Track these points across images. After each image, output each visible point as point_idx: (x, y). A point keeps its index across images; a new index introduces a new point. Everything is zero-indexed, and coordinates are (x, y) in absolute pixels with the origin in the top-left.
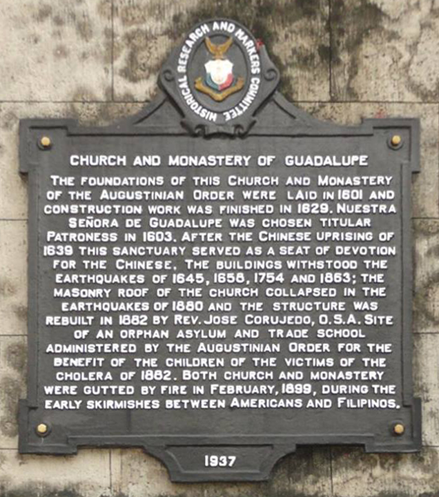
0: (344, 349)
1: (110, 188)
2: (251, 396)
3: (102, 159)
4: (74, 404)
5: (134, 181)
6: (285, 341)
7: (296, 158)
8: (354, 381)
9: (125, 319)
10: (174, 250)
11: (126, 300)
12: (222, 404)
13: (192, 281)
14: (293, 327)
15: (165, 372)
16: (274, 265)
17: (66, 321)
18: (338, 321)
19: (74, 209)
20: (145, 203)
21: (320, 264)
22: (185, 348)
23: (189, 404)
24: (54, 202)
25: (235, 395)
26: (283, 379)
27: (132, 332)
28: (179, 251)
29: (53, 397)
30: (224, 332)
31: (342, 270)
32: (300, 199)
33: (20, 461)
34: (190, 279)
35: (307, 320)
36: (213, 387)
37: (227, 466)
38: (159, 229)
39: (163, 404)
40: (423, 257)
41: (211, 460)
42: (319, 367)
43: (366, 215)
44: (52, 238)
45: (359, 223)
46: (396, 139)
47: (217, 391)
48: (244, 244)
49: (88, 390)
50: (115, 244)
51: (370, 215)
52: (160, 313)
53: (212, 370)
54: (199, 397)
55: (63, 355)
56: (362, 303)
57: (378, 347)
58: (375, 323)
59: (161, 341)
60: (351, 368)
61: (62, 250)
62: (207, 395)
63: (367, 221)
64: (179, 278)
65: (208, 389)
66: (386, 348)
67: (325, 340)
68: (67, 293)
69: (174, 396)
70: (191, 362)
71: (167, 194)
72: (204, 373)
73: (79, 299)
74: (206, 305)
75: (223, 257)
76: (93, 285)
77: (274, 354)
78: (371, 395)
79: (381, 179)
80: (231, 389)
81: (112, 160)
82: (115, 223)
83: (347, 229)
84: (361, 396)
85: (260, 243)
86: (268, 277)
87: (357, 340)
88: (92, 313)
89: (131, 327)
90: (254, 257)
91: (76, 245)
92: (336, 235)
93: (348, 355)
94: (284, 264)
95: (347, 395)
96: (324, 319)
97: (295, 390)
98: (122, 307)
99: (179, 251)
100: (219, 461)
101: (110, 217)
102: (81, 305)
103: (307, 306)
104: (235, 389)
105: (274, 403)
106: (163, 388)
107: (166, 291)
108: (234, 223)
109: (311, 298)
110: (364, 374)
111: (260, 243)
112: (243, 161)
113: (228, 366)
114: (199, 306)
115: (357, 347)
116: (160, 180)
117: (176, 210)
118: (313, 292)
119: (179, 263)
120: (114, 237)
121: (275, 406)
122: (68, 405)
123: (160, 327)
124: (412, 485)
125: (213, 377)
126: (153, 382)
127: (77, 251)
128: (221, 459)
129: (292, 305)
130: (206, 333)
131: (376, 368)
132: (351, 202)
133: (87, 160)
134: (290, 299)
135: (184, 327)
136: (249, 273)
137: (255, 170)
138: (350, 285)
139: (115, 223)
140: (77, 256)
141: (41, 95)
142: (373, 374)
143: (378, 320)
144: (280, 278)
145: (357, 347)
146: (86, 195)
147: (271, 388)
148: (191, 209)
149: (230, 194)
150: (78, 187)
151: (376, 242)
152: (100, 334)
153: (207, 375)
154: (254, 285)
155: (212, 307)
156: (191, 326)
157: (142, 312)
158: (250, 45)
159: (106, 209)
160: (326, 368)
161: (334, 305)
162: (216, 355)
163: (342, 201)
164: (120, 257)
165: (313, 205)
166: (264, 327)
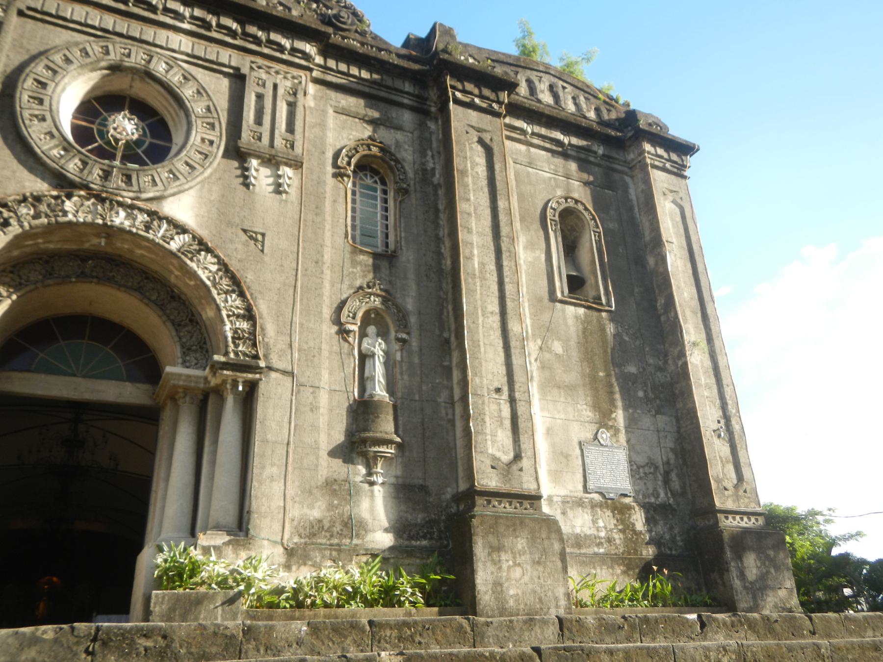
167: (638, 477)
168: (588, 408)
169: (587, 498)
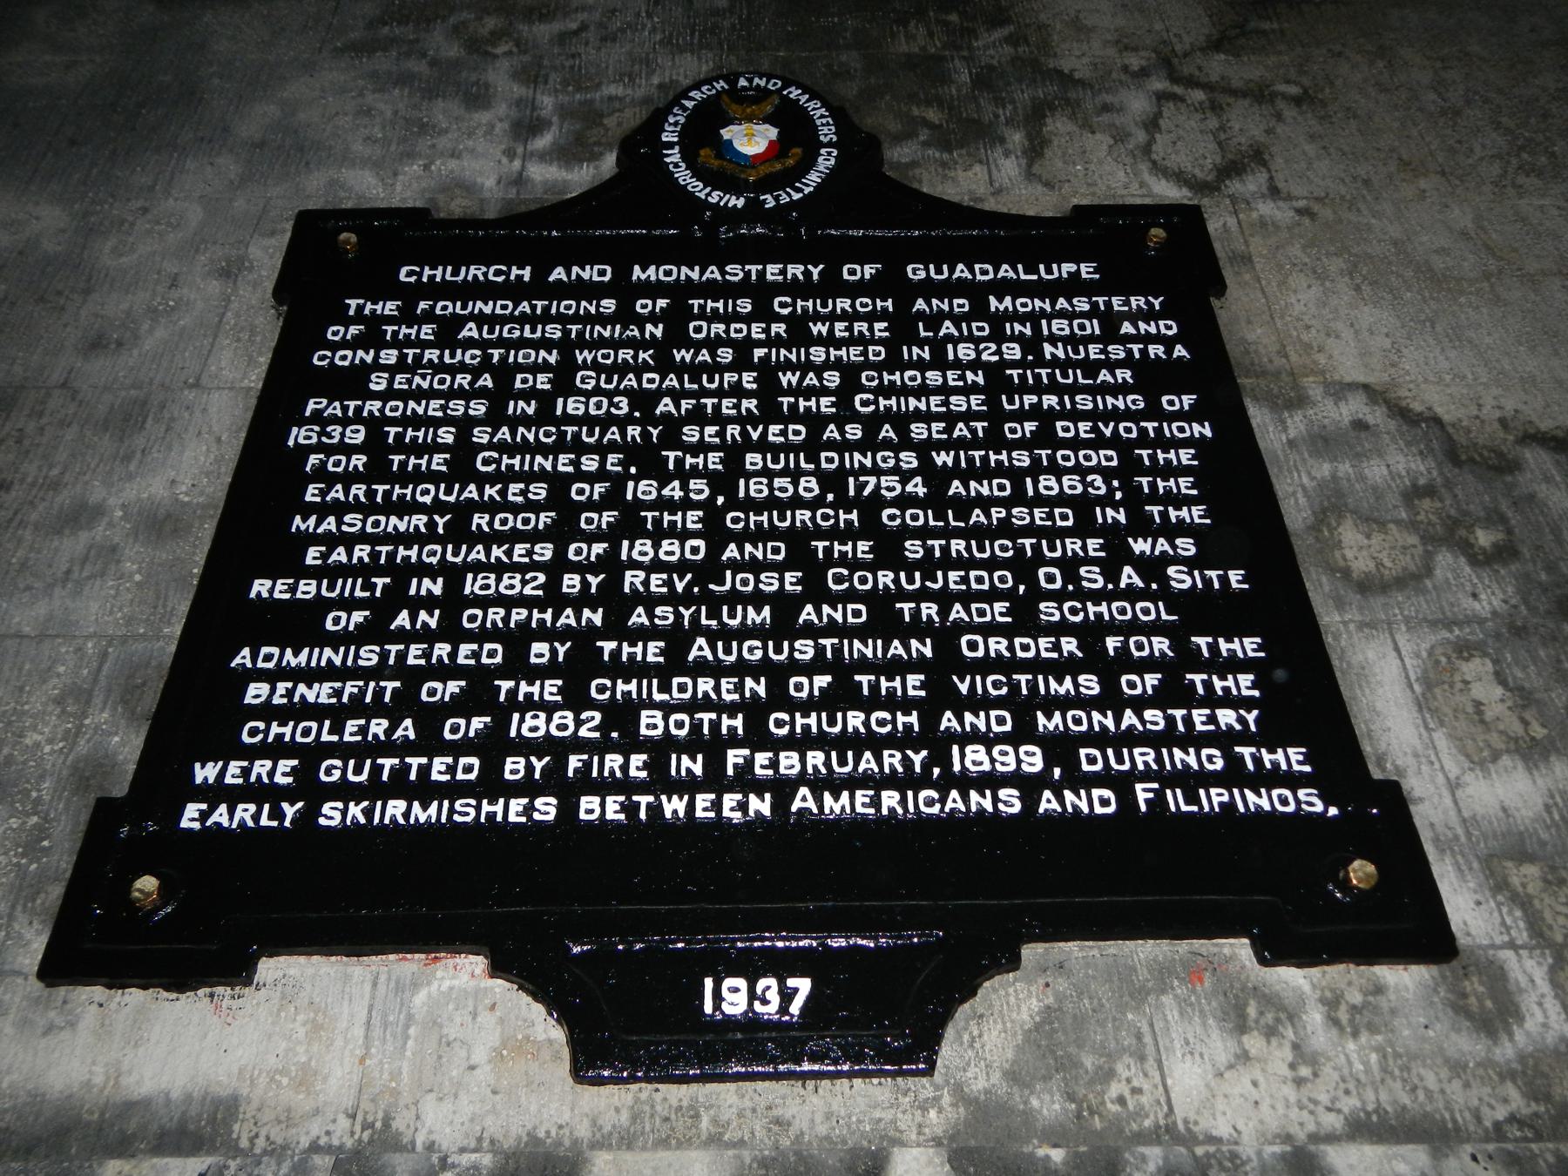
1: (481, 319)
2: (854, 783)
3: (475, 271)
4: (277, 814)
6: (947, 636)
12: (761, 805)
14: (967, 598)
15: (584, 716)
16: (898, 460)
17: (307, 589)
19: (390, 356)
21: (1022, 459)
22: (653, 652)
25: (802, 779)
27: (496, 615)
29: (218, 794)
30: (766, 611)
34: (674, 490)
35: (1004, 579)
36: (734, 757)
38: (597, 391)
39: (568, 809)
41: (725, 993)
42: (1057, 696)
44: (317, 414)
45: (1104, 376)
48: (815, 422)
49: (331, 771)
51: (1127, 362)
52: (581, 569)
53: (732, 710)
54: (689, 786)
55: (281, 673)
57: (1224, 646)
59: (584, 639)
60: (1159, 699)
61: (337, 435)
62: (715, 780)
63: (1124, 375)
65: (715, 763)
66: (1249, 646)
67: (1062, 628)
68: (330, 524)
69: (603, 787)
73: (363, 537)
74: (715, 549)
75: (763, 446)
76: (405, 508)
77: (918, 665)
78: (1234, 776)
80: (789, 762)
82: (487, 381)
84: (1208, 779)
85: (856, 417)
86: (884, 484)
87: (1155, 629)
88: (391, 568)
90: (843, 446)
91: (375, 426)
92: (1050, 400)
96: (1050, 579)
97: (993, 761)
98: (478, 554)
99: (645, 435)
102: (362, 552)
103: (1001, 548)
104: (803, 761)
106: (574, 762)
107: (608, 517)
108: (788, 379)
109: (1006, 529)
110: (1199, 716)
111: (856, 417)
112: (807, 273)
113: (779, 698)
115: (1161, 644)
116: (609, 305)
119: (646, 460)
120: (479, 408)
123: (583, 600)
128: (759, 990)
129: (958, 545)
130: (714, 613)
131: (1229, 701)
132: (1072, 341)
134: (948, 534)
135: (650, 602)
137: (831, 286)
138: (1107, 501)
140: (375, 446)
142: (1226, 717)
144: (917, 487)
145: (1161, 644)
146: (427, 332)
147: (918, 759)
149: (779, 328)
150: (407, 316)
152: (403, 619)
154: (843, 503)
155: (731, 551)
156: (672, 599)
159: (471, 356)
161: (1073, 545)
162: (742, 669)
165: (982, 346)
166: (880, 603)
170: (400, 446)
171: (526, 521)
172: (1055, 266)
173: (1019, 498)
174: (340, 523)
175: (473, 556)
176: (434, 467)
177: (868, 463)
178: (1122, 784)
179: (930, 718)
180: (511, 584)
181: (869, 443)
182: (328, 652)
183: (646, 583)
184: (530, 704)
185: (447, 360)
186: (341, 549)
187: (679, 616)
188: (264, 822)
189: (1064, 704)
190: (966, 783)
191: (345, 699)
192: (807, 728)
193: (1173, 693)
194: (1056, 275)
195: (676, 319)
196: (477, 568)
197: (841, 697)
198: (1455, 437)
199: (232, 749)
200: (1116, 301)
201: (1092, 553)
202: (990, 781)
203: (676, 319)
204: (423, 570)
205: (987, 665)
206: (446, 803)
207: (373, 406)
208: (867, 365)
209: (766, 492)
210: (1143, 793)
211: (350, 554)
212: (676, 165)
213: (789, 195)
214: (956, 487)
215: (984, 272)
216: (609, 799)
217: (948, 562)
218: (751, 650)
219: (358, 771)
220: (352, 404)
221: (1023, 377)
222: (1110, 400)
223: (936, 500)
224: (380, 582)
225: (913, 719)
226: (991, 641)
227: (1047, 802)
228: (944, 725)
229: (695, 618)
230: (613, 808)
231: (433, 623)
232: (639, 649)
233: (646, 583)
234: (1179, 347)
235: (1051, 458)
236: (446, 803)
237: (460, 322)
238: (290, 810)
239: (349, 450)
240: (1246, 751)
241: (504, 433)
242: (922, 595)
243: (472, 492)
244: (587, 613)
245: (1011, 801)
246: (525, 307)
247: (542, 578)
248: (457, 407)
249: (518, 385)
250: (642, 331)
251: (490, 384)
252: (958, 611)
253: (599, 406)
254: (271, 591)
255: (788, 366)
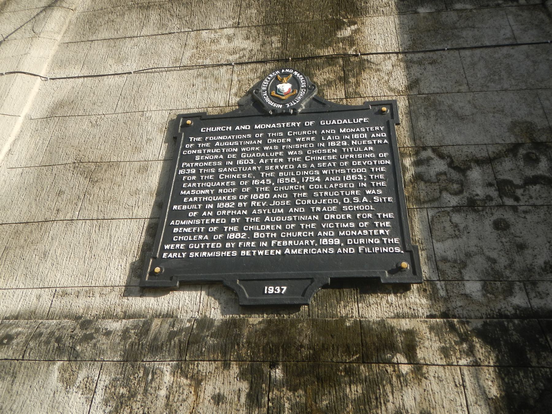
0: (361, 217)
1: (220, 141)
2: (298, 247)
3: (218, 129)
4: (181, 255)
5: (235, 137)
6: (321, 214)
7: (327, 121)
8: (369, 236)
9: (220, 205)
10: (254, 168)
11: (223, 194)
12: (279, 252)
13: (264, 183)
14: (327, 205)
15: (242, 234)
16: (314, 173)
17: (185, 207)
18: (356, 201)
19: (200, 151)
20: (239, 147)
22: (257, 219)
23: (257, 253)
24: (189, 149)
26: (320, 236)
27: (224, 212)
28: (257, 169)
29: (169, 251)
30: (282, 210)
31: (357, 173)
32: (329, 140)
33: (141, 294)
34: (263, 182)
36: (273, 242)
37: (281, 293)
38: (246, 158)
40: (409, 167)
41: (269, 289)
42: (345, 228)
43: (370, 145)
45: (366, 149)
46: (384, 109)
47: (276, 245)
48: (296, 163)
49: (191, 246)
50: (220, 167)
52: (243, 201)
54: (264, 248)
55: (180, 226)
56: (371, 191)
58: (381, 201)
59: (243, 216)
60: (367, 228)
61: (189, 171)
62: (270, 247)
63: (371, 148)
64: (256, 182)
65: (270, 244)
66: (390, 215)
67: (348, 212)
68: (189, 192)
69: (246, 249)
70: (260, 228)
71: (253, 142)
72: (268, 234)
73: (195, 195)
75: (284, 170)
76: (205, 188)
77: (315, 221)
78: (382, 244)
79: (377, 128)
80: (285, 243)
81: (224, 128)
82: (222, 157)
83: (359, 152)
84: (375, 245)
85: (305, 162)
86: (310, 179)
89: (225, 209)
90: (302, 169)
91: (197, 168)
92: (352, 156)
93: (363, 220)
94: (321, 172)
95: (366, 245)
96: (346, 200)
97: (328, 242)
98: (220, 198)
99: (257, 169)
100: (275, 290)
101: (219, 154)
102: (196, 199)
104: (288, 243)
105: (314, 251)
106: (240, 244)
107: (248, 190)
108: (291, 153)
110: (375, 231)
111: (305, 162)
112: (296, 125)
113: (284, 229)
114: (267, 196)
115: (370, 215)
116: (249, 136)
117: (257, 149)
118: (339, 185)
120: (220, 163)
121: (315, 253)
122: (177, 256)
123: (243, 208)
124: (420, 309)
125: (273, 236)
126: (235, 240)
127: (198, 171)
128: (276, 289)
129: (326, 193)
130: (271, 211)
131: (384, 228)
132: (360, 139)
133: (211, 129)
134: (324, 190)
135: (256, 208)
136: (299, 178)
137: (303, 128)
138: (363, 181)
139: (222, 157)
140: (198, 174)
141: (191, 105)
142: (382, 232)
143: (383, 200)
144: (318, 179)
146: (207, 145)
147: (312, 242)
148: (266, 148)
149: (289, 140)
150: (204, 141)
151: (378, 158)
152: (205, 214)
153: (270, 235)
154: (301, 183)
155: (275, 196)
156: (262, 207)
157: (232, 201)
158: (301, 78)
159: (216, 151)
160: (350, 229)
161: (353, 192)
162: (276, 223)
163: (354, 139)
164: (222, 173)
166: (308, 207)
167: (454, 201)
168: (241, 33)
169: (126, 316)
170: (203, 174)
171: (230, 190)
172: (357, 119)
173: (342, 181)
174: (191, 192)
175: (219, 199)
176: (210, 178)
177: (307, 174)
178: (356, 246)
179: (316, 234)
180: (228, 205)
181: (309, 169)
182: (189, 221)
183: (256, 204)
184: (232, 232)
185: (212, 152)
186: (191, 198)
187: (263, 212)
188: (179, 256)
189: (346, 229)
190: (323, 246)
191: (194, 231)
192: (289, 235)
193: (372, 226)
194: (357, 122)
195: (265, 139)
196: (220, 201)
197: (298, 228)
198: (454, 160)
199: (172, 242)
200: (371, 128)
201: (357, 194)
202: (328, 246)
203: (265, 139)
204: (209, 202)
205: (330, 221)
206: (214, 253)
207: (197, 164)
208: (309, 148)
209: (283, 182)
210: (360, 249)
211: (193, 199)
212: (266, 96)
213: (293, 103)
214: (327, 179)
215: (340, 122)
216: (247, 251)
217: (324, 197)
218: (279, 218)
219: (197, 246)
220: (192, 164)
221: (346, 150)
222: (366, 155)
223: (323, 182)
224: (200, 205)
225: (312, 233)
226: (331, 215)
227: (339, 250)
228: (319, 234)
229: (267, 211)
230: (248, 253)
231: (211, 214)
232: (254, 219)
233: (256, 204)
234: (385, 140)
235: (350, 171)
236: (214, 253)
237: (215, 141)
238: (184, 254)
239: (191, 175)
240: (385, 239)
241: (225, 169)
242: (318, 205)
243: (219, 184)
244: (243, 211)
245: (332, 250)
246: (230, 137)
247: (234, 204)
248: (215, 163)
249: (228, 157)
250: (257, 142)
251: (222, 157)
252: (324, 209)
253: (246, 162)
254: (177, 208)
255: (291, 150)
